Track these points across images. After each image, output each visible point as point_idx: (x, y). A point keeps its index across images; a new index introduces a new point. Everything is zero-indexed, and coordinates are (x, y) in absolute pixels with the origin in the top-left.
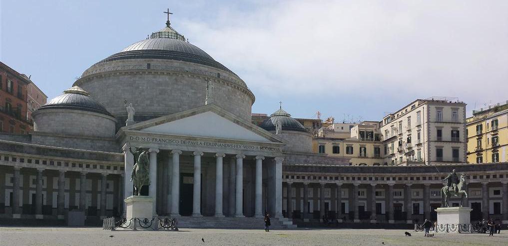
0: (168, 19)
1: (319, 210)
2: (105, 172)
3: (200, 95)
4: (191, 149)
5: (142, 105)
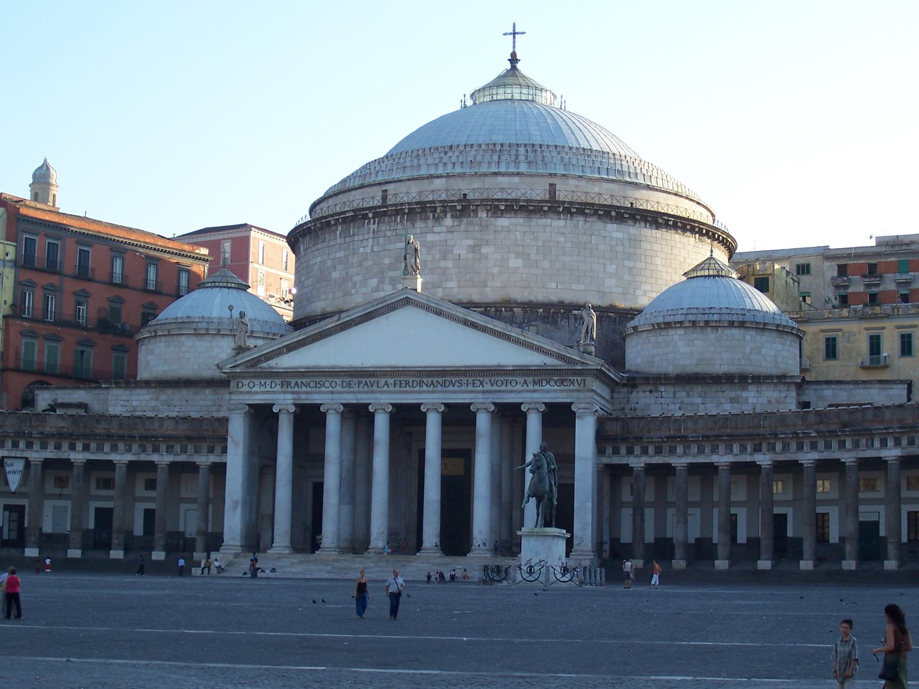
0: (514, 47)
4: (363, 398)
5: (363, 290)
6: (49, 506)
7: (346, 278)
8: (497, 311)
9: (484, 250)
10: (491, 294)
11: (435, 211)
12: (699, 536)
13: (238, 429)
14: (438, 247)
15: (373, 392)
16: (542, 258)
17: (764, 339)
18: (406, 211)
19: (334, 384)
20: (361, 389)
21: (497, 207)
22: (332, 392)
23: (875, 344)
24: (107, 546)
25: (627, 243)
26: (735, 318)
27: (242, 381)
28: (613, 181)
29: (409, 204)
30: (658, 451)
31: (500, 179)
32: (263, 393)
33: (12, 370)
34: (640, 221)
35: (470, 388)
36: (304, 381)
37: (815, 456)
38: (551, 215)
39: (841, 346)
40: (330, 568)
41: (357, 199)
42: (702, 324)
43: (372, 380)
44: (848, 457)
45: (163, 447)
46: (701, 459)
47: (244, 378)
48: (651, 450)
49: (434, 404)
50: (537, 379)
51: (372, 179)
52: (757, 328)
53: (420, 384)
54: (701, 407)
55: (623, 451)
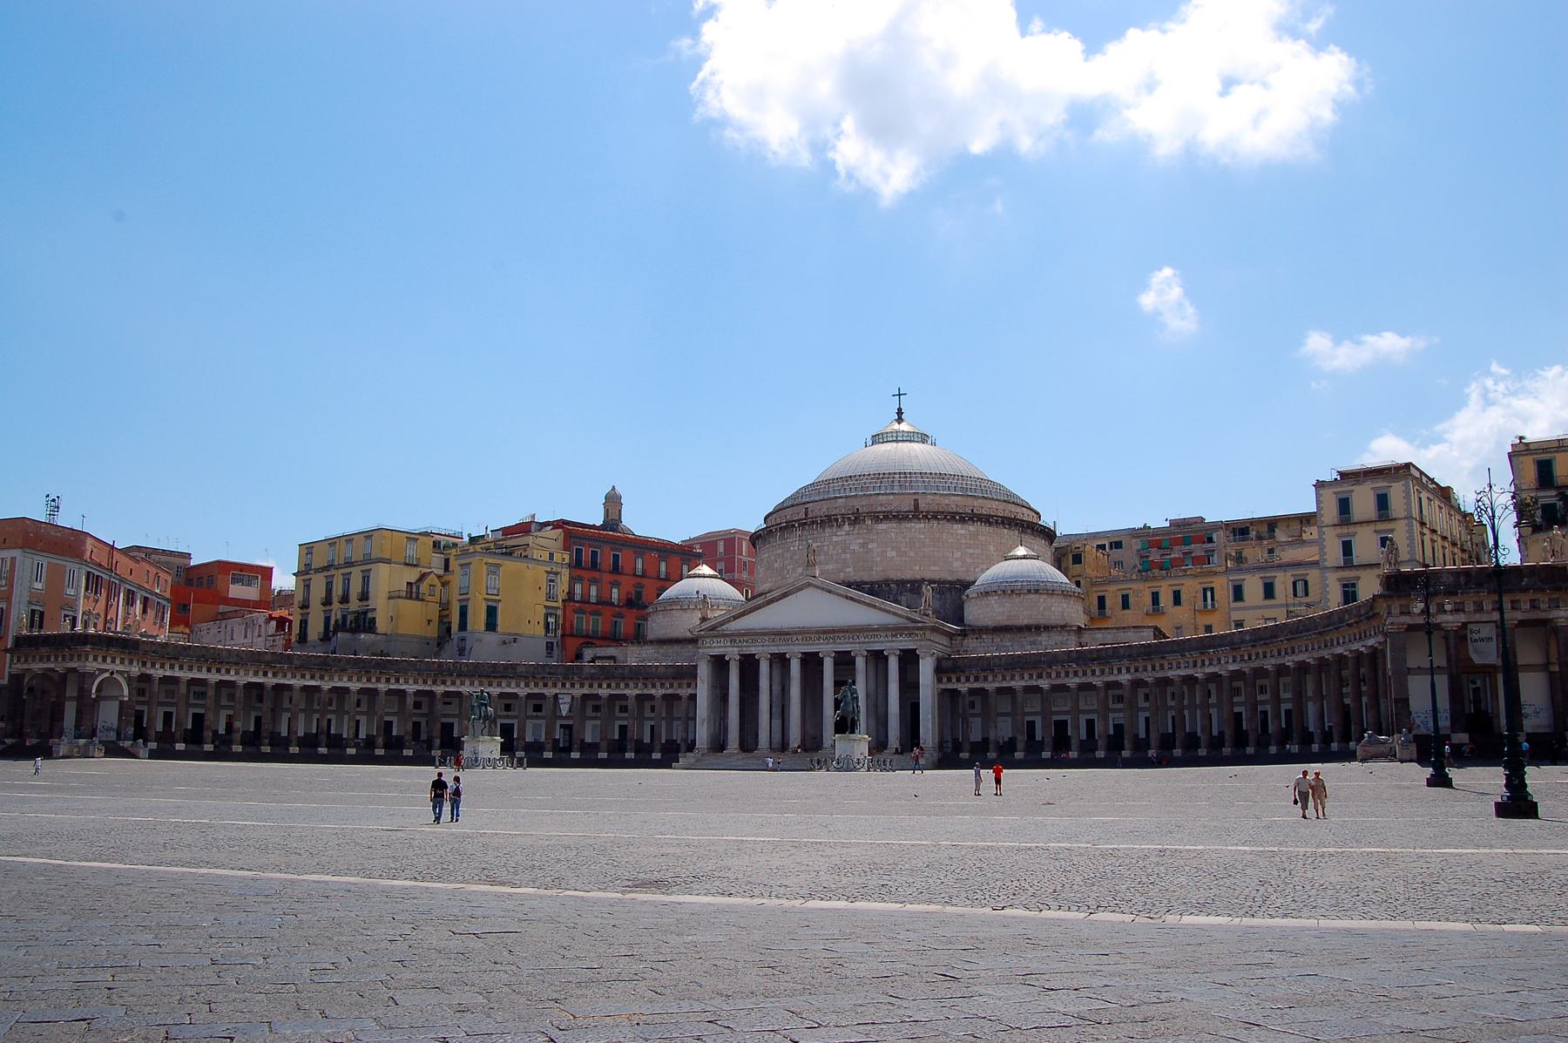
1: (1171, 731)
2: (685, 691)
3: (875, 545)
4: (782, 649)
6: (589, 725)
7: (784, 567)
8: (879, 587)
9: (869, 547)
10: (875, 575)
12: (1010, 736)
13: (704, 672)
16: (909, 549)
17: (1053, 600)
21: (878, 517)
23: (1155, 598)
24: (623, 750)
25: (968, 538)
26: (1032, 588)
28: (958, 495)
30: (977, 679)
31: (880, 497)
33: (568, 635)
34: (977, 521)
37: (1077, 680)
38: (915, 521)
39: (1131, 600)
40: (760, 762)
41: (789, 515)
42: (1009, 592)
44: (1097, 681)
45: (658, 685)
46: (1005, 684)
47: (707, 637)
48: (972, 679)
49: (827, 652)
51: (800, 500)
52: (1047, 594)
54: (1010, 648)
55: (954, 680)
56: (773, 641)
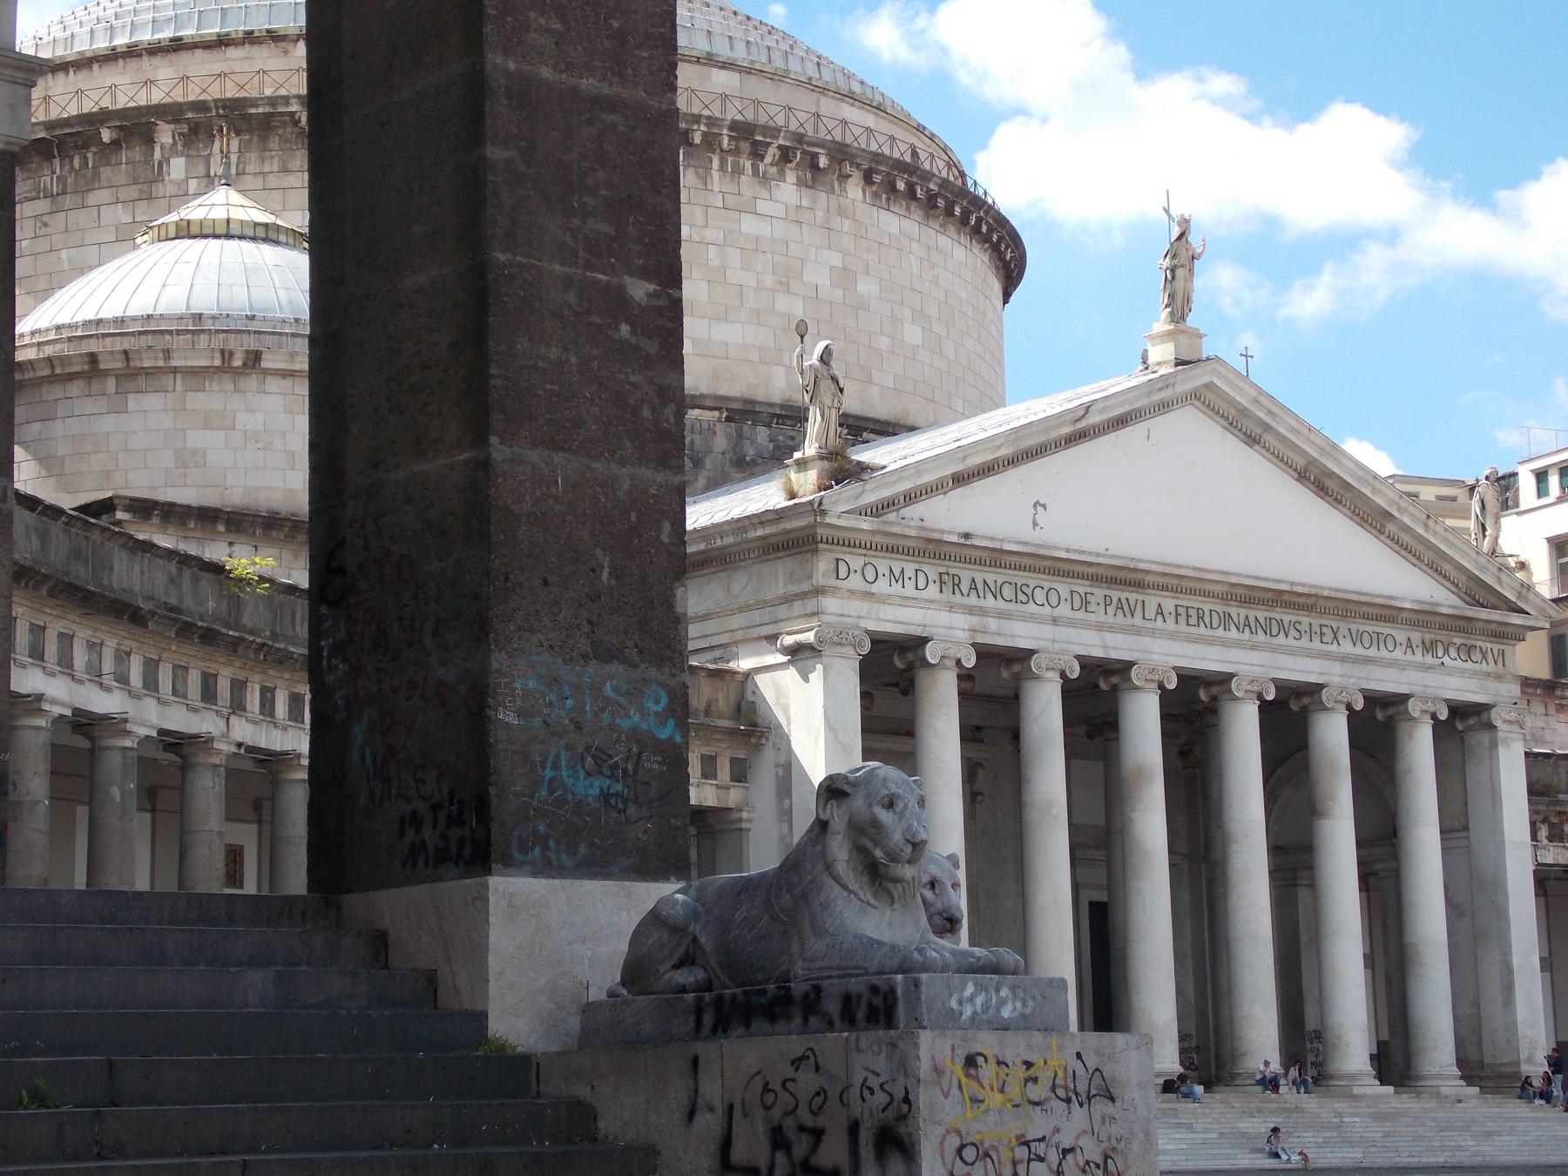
11: (762, 158)
14: (769, 256)
15: (1137, 631)
18: (697, 140)
19: (1054, 599)
20: (1111, 619)
22: (1055, 621)
27: (847, 558)
29: (711, 121)
32: (905, 600)
35: (1316, 644)
36: (990, 578)
43: (1133, 597)
50: (1428, 637)
53: (1226, 621)
56: (1085, 603)
